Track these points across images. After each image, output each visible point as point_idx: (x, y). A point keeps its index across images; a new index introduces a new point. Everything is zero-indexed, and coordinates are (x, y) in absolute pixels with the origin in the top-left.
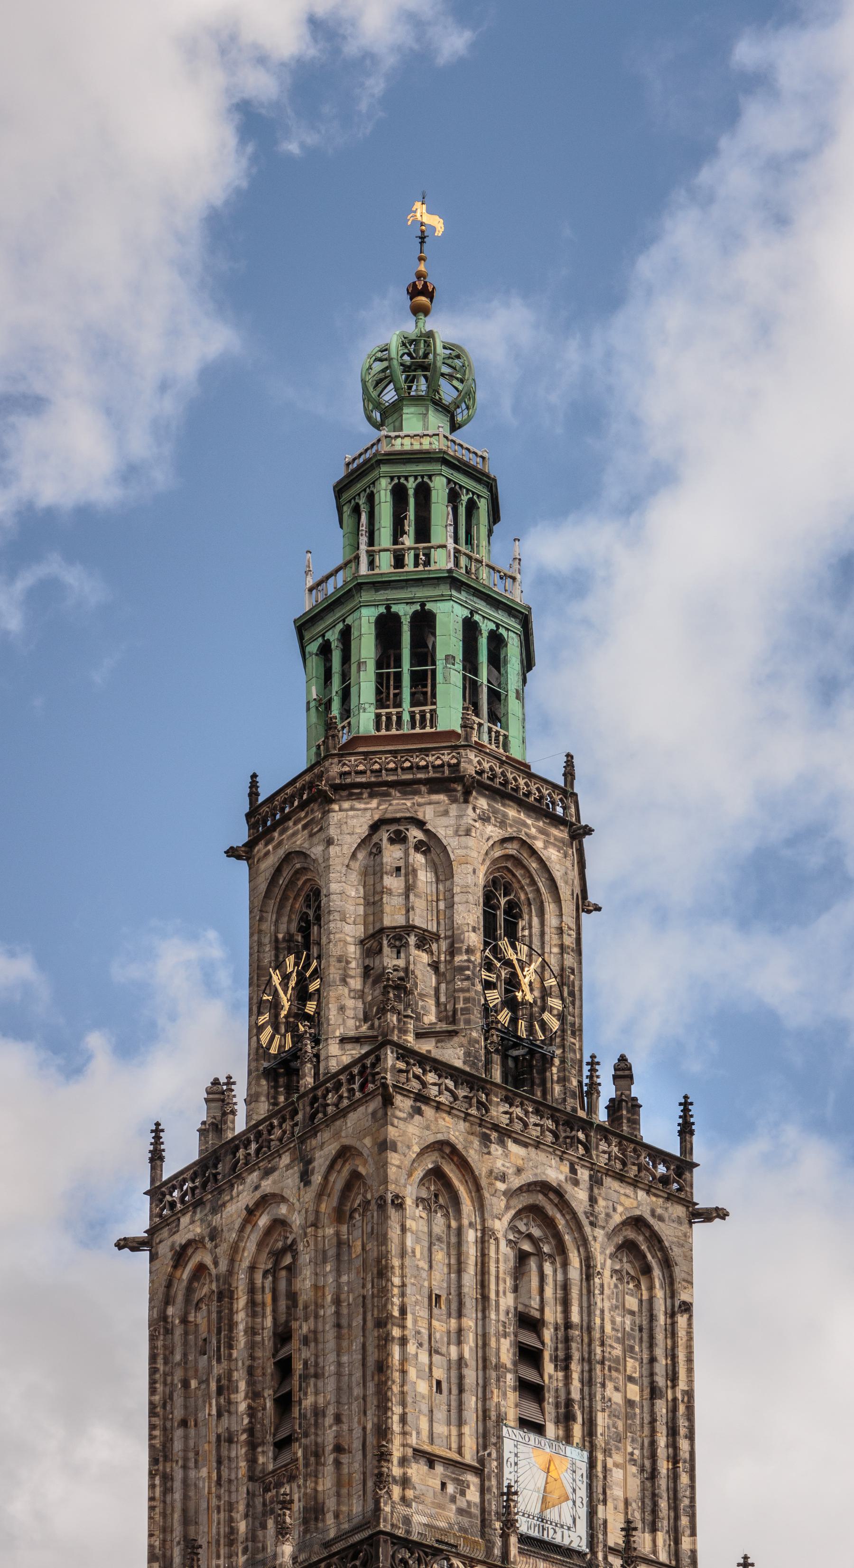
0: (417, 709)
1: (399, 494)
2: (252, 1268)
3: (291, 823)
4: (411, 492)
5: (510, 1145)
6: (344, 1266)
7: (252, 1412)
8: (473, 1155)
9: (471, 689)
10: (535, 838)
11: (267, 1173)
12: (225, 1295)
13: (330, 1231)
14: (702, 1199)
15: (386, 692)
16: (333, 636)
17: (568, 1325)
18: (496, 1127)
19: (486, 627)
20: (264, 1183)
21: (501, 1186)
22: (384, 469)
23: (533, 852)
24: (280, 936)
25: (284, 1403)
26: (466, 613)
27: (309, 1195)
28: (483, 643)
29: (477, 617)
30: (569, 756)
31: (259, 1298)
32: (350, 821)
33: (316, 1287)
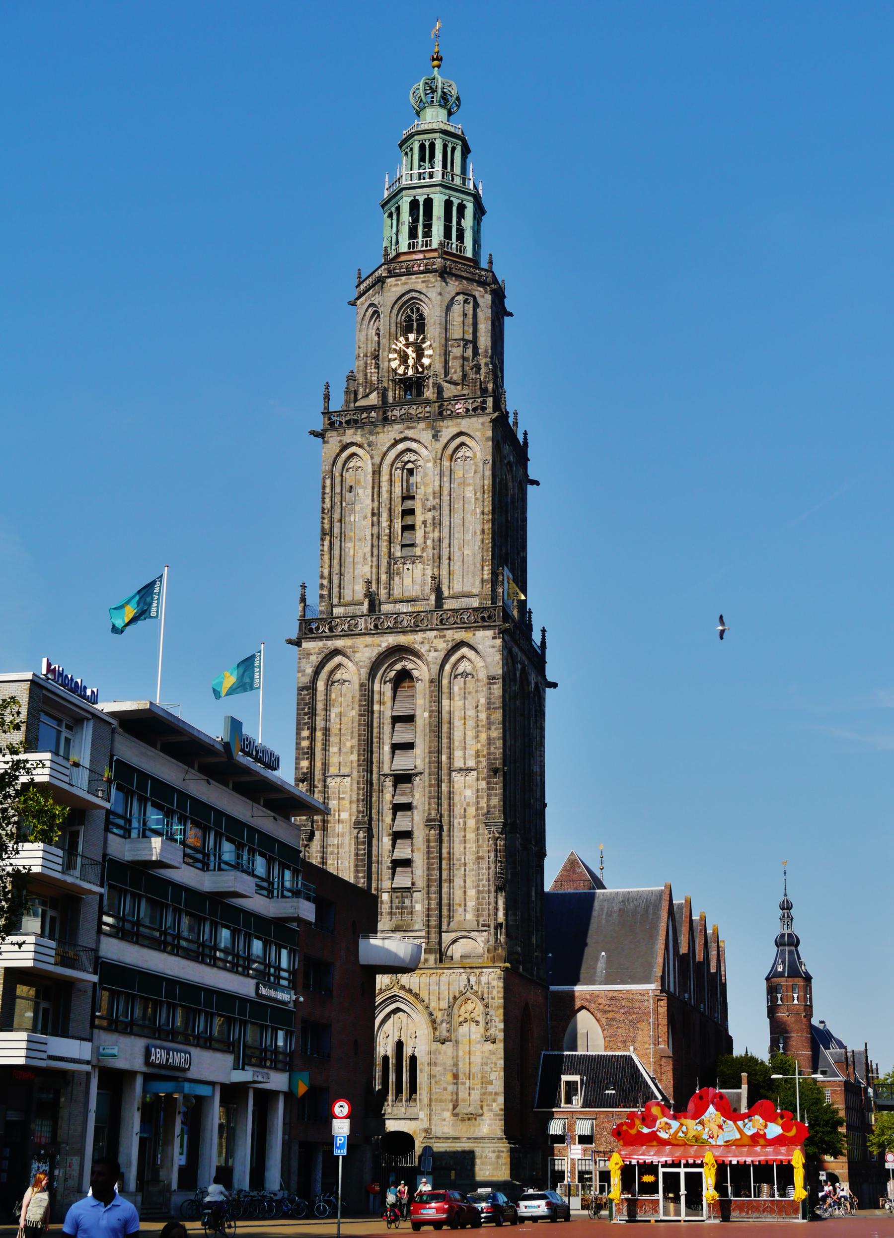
2: (392, 465)
3: (414, 277)
7: (390, 527)
11: (409, 428)
14: (532, 476)
16: (421, 200)
17: (507, 521)
20: (406, 432)
25: (408, 528)
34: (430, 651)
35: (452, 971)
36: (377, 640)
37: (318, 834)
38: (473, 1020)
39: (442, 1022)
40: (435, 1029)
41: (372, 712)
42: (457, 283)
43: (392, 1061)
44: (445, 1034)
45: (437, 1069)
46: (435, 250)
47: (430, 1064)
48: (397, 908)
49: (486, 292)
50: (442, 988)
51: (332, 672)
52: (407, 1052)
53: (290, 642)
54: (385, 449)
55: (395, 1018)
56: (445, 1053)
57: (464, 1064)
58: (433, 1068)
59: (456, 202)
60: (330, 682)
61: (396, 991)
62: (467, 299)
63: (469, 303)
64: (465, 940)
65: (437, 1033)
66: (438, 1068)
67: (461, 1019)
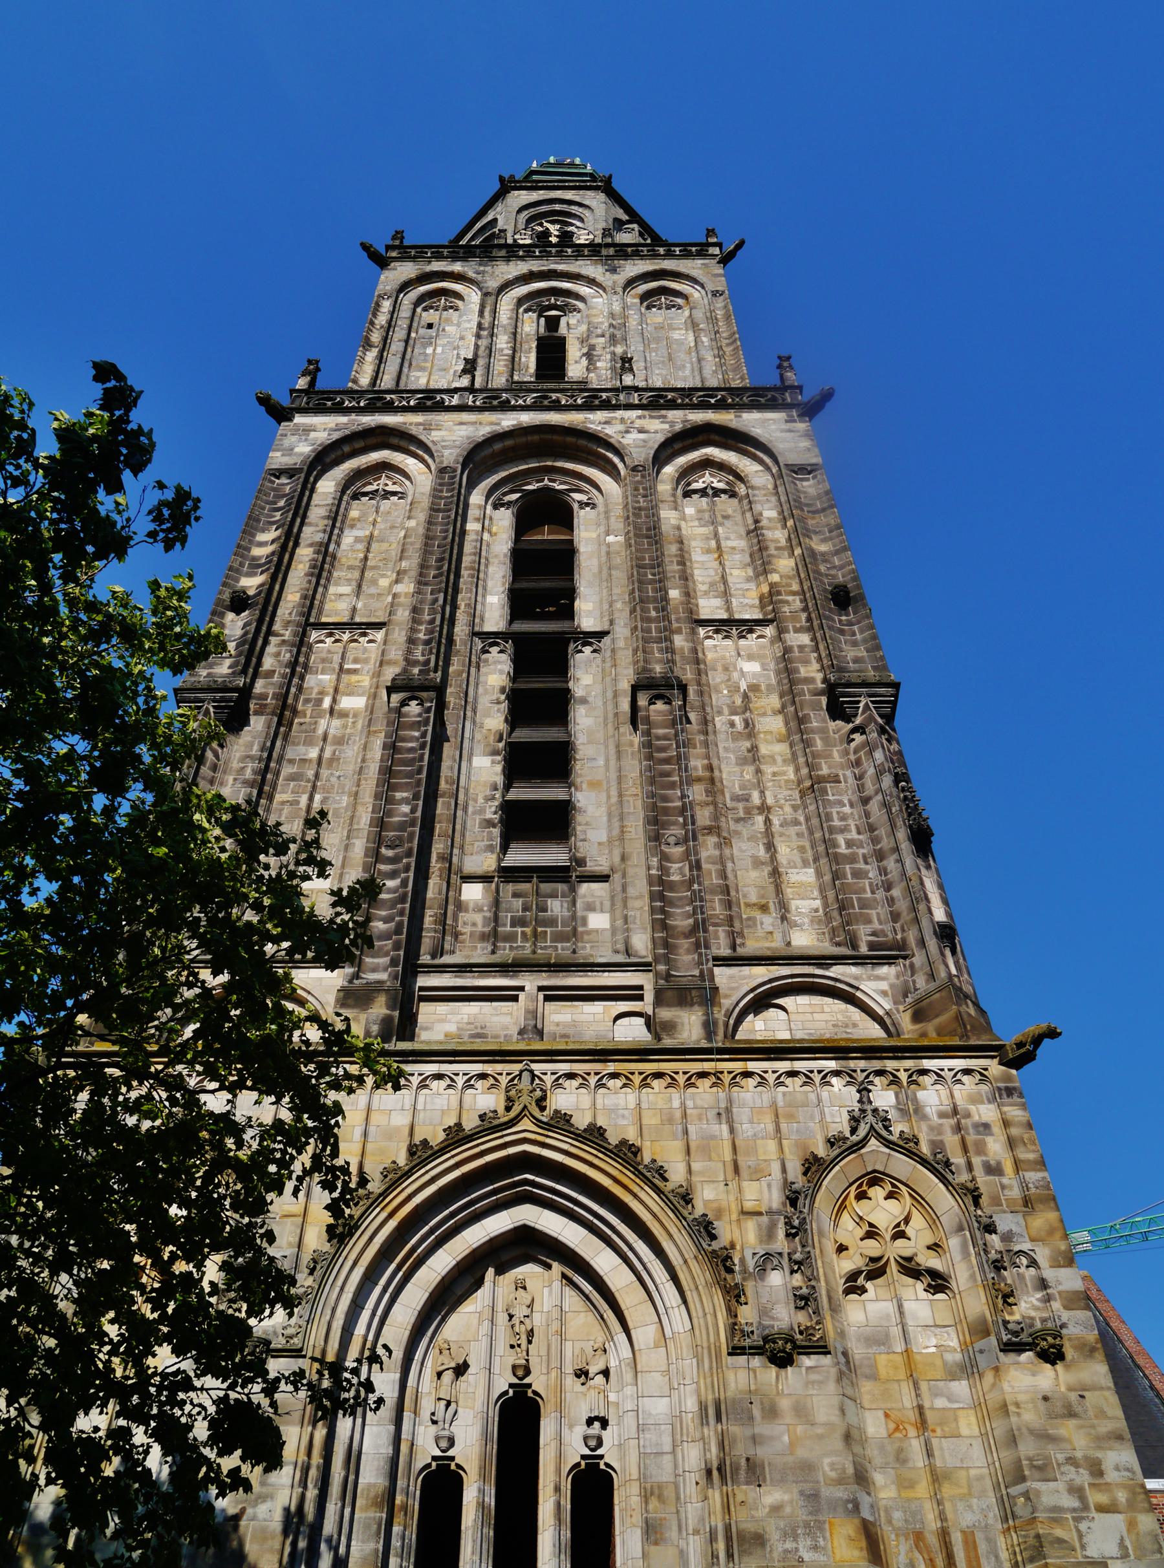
34: (627, 432)
35: (784, 1066)
36: (487, 417)
37: (257, 724)
38: (910, 1268)
39: (767, 1261)
40: (734, 1295)
41: (463, 532)
43: (476, 1497)
44: (785, 1317)
45: (768, 1501)
47: (719, 1472)
48: (517, 922)
50: (745, 1129)
51: (359, 474)
52: (559, 1448)
53: (264, 401)
55: (496, 1289)
56: (802, 1412)
57: (904, 1484)
58: (744, 1491)
60: (352, 488)
61: (527, 1136)
64: (803, 1000)
65: (747, 1314)
66: (771, 1496)
67: (847, 1265)
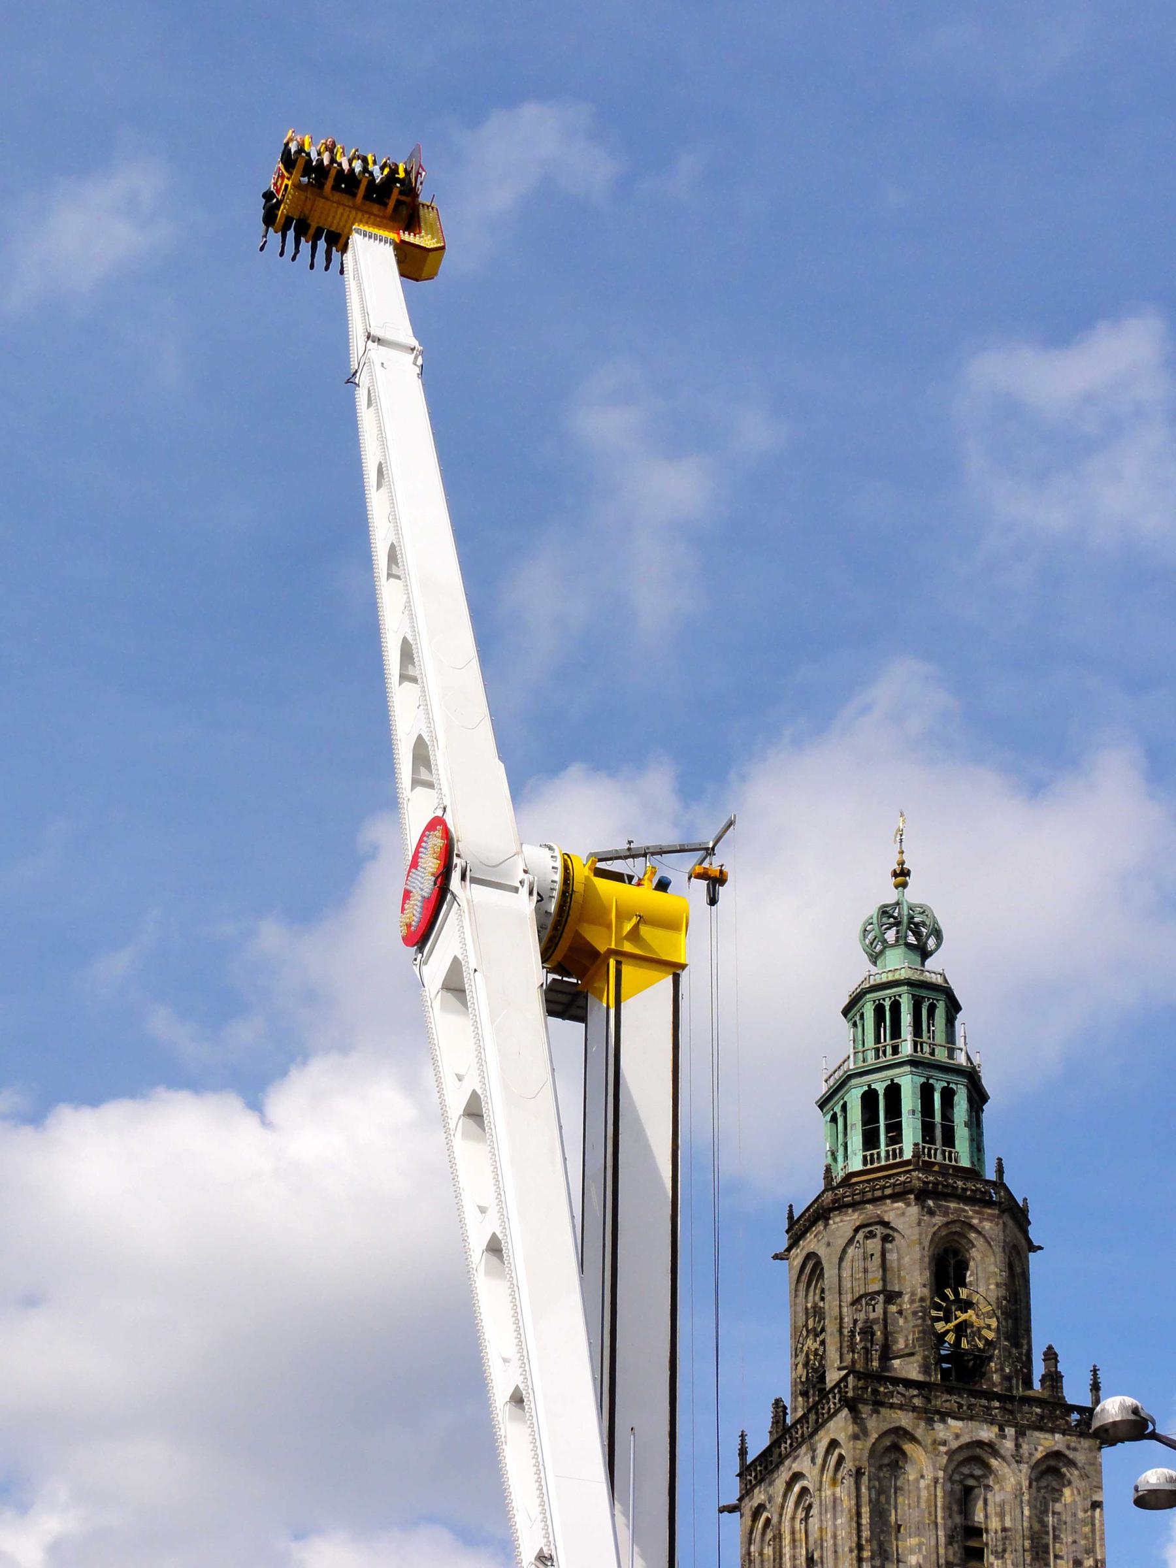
0: (890, 1148)
1: (879, 1010)
2: (793, 1518)
4: (887, 1008)
5: (950, 1421)
6: (838, 1514)
8: (919, 1433)
9: (927, 1129)
10: (972, 1218)
12: (778, 1537)
13: (829, 1493)
15: (870, 1140)
16: (838, 1109)
18: (938, 1412)
19: (939, 1086)
21: (943, 1449)
22: (868, 996)
23: (972, 1227)
24: (809, 1305)
26: (923, 1080)
27: (816, 1470)
28: (937, 1097)
29: (931, 1081)
30: (1000, 1160)
31: (797, 1536)
32: (843, 1224)
33: (821, 1529)
42: (856, 1216)
46: (908, 1163)
49: (908, 1205)
54: (780, 1500)
59: (880, 1088)
62: (871, 1232)
63: (874, 1236)
